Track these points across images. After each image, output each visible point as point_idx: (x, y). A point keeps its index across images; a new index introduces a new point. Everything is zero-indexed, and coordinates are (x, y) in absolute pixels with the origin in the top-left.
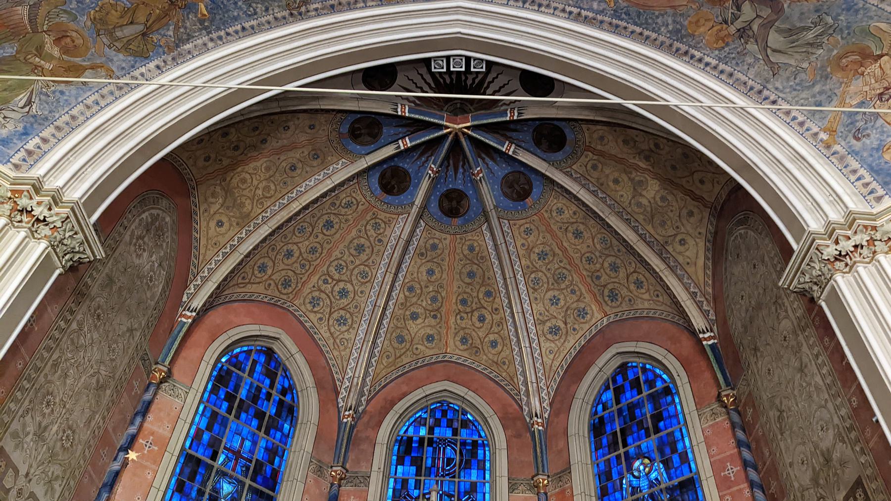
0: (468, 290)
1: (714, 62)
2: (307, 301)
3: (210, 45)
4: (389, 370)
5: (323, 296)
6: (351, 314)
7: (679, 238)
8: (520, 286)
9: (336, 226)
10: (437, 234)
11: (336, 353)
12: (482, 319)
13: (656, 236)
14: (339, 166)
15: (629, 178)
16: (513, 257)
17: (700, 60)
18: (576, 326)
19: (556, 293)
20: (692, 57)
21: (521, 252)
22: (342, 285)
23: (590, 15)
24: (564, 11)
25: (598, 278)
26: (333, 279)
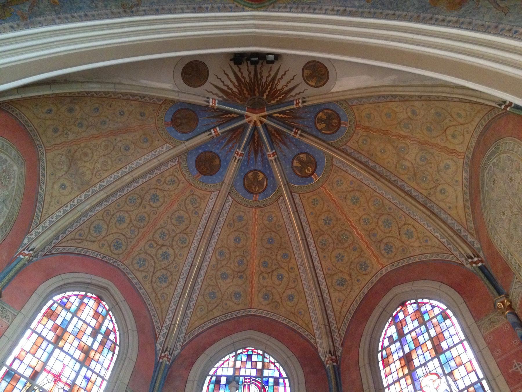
0: (269, 254)
1: (455, 19)
2: (135, 262)
4: (202, 321)
5: (149, 258)
6: (171, 273)
7: (440, 188)
8: (311, 247)
9: (161, 200)
10: (243, 208)
11: (157, 305)
12: (280, 277)
13: (421, 191)
14: (164, 149)
15: (393, 147)
16: (304, 224)
17: (443, 20)
18: (359, 278)
19: (341, 251)
20: (436, 20)
21: (311, 219)
22: (164, 249)
23: (354, 9)
24: (333, 10)
25: (375, 235)
26: (157, 244)
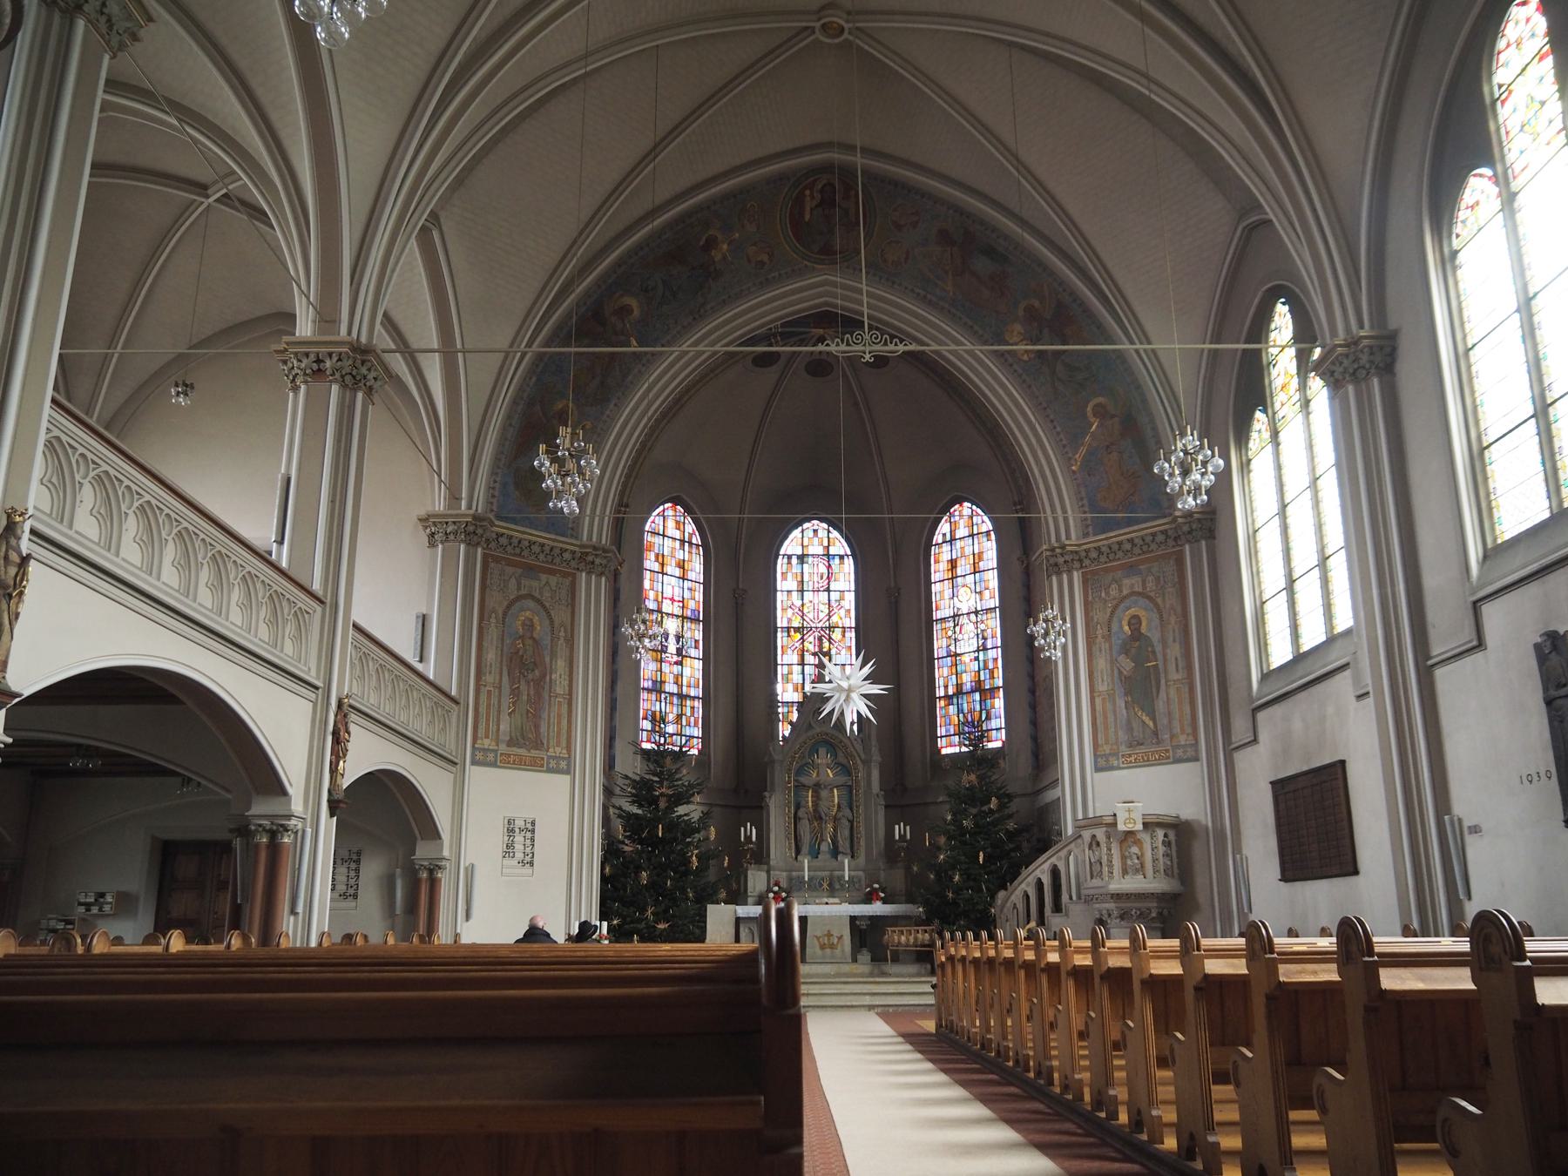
1: (1020, 371)
3: (644, 369)
20: (1006, 360)
23: (934, 299)
24: (912, 291)
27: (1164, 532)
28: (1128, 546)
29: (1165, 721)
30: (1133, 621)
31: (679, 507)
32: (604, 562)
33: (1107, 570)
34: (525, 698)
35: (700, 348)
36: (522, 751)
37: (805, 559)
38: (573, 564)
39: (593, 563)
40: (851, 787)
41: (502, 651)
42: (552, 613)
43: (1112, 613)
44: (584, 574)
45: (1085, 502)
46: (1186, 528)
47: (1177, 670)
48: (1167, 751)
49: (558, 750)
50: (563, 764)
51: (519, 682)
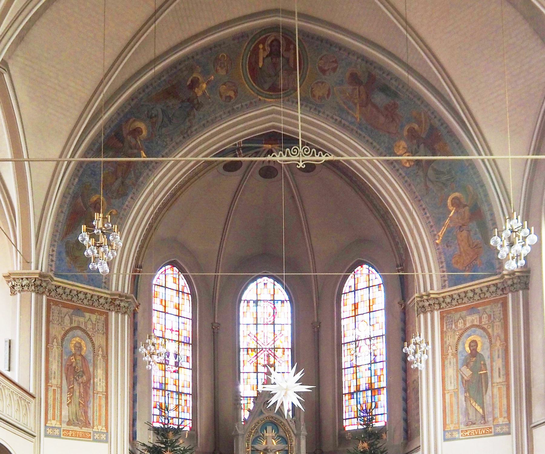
20: (394, 167)
23: (347, 123)
24: (332, 118)
27: (495, 285)
28: (471, 294)
29: (490, 409)
30: (472, 344)
31: (175, 268)
32: (127, 305)
33: (456, 310)
34: (77, 394)
35: (188, 158)
36: (77, 429)
37: (259, 303)
38: (106, 306)
39: (119, 305)
40: (287, 451)
41: (62, 363)
42: (94, 339)
43: (459, 339)
44: (113, 313)
45: (444, 264)
46: (510, 282)
47: (499, 376)
48: (490, 428)
49: (100, 427)
50: (103, 437)
51: (73, 384)
